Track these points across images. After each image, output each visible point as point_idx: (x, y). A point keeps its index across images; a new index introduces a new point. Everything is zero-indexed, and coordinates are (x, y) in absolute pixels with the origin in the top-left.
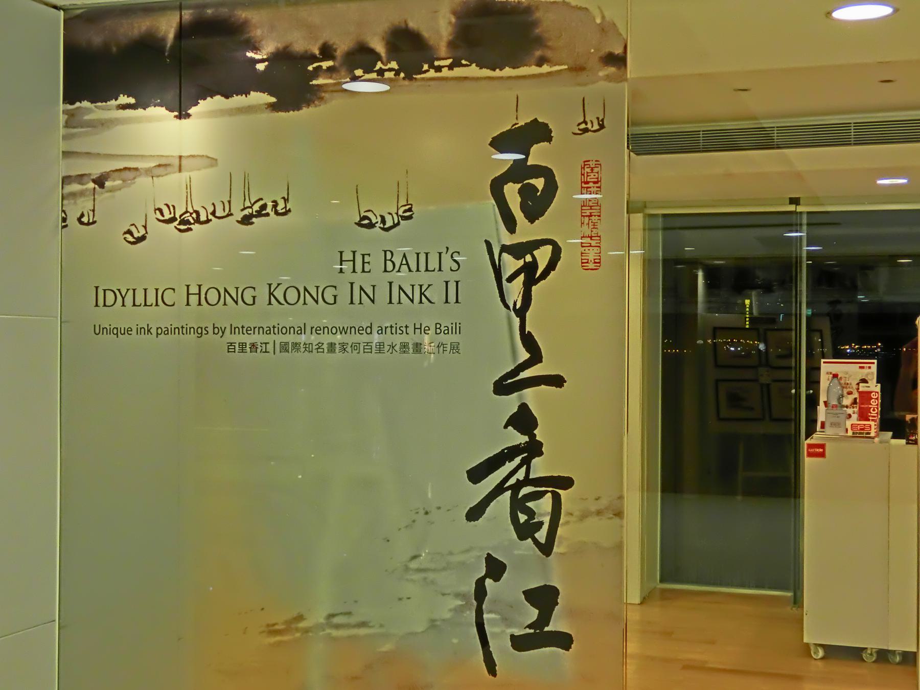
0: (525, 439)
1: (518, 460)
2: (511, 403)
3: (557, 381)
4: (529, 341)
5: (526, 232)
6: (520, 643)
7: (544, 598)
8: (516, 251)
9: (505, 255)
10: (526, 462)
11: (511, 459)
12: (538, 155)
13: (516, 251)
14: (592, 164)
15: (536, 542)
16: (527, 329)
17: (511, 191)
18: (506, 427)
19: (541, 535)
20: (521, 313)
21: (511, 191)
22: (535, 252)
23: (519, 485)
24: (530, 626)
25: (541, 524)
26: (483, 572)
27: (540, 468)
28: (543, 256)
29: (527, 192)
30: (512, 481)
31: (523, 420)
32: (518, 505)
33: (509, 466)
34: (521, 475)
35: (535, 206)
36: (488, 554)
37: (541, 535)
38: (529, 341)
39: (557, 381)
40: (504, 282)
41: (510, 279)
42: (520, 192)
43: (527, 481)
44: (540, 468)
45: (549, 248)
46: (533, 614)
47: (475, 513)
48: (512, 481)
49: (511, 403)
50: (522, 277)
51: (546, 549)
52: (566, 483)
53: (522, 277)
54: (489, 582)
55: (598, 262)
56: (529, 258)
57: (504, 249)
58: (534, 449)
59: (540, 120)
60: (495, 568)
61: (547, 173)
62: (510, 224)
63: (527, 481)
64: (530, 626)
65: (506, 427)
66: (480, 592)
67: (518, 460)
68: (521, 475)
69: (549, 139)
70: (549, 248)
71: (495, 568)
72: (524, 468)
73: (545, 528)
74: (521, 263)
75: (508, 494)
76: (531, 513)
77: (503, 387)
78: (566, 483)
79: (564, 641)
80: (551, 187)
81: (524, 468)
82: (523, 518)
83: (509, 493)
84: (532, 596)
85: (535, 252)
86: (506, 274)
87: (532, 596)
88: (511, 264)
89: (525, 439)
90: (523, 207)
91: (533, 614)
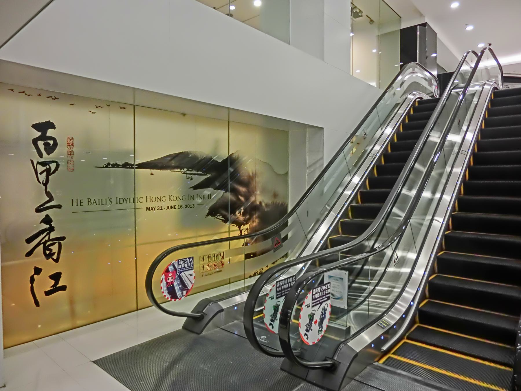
0: (48, 226)
1: (45, 234)
2: (43, 214)
3: (59, 207)
4: (48, 194)
5: (46, 157)
6: (48, 293)
7: (56, 277)
8: (43, 164)
9: (38, 165)
10: (49, 234)
11: (43, 234)
12: (50, 132)
13: (43, 164)
14: (71, 138)
15: (53, 259)
16: (48, 190)
17: (41, 144)
18: (40, 223)
19: (55, 257)
20: (45, 185)
21: (41, 144)
22: (50, 165)
23: (46, 241)
24: (51, 287)
25: (55, 253)
26: (33, 273)
27: (53, 235)
28: (53, 166)
29: (46, 145)
30: (44, 241)
31: (47, 220)
32: (46, 248)
33: (42, 236)
34: (47, 238)
35: (50, 149)
36: (35, 267)
37: (55, 257)
38: (48, 194)
39: (59, 207)
40: (39, 175)
41: (41, 173)
42: (44, 144)
43: (49, 240)
44: (53, 235)
45: (55, 164)
46: (53, 282)
47: (29, 254)
48: (44, 241)
49: (43, 214)
50: (45, 173)
51: (57, 261)
52: (63, 238)
53: (45, 173)
54: (35, 276)
55: (73, 169)
56: (48, 167)
57: (38, 163)
58: (51, 229)
59: (51, 121)
60: (38, 271)
61: (54, 139)
62: (41, 155)
63: (49, 240)
64: (51, 287)
65: (40, 223)
66: (32, 280)
67: (45, 234)
68: (47, 238)
69: (55, 128)
70: (55, 164)
71: (38, 271)
72: (48, 236)
73: (56, 255)
74: (45, 168)
75: (42, 245)
76: (51, 250)
77: (38, 210)
78: (63, 238)
79: (64, 288)
80: (55, 144)
81: (48, 236)
82: (48, 252)
83: (42, 245)
84: (52, 277)
85: (50, 165)
86: (39, 172)
87: (52, 277)
88: (40, 168)
89: (48, 226)
90: (45, 149)
91: (53, 282)
